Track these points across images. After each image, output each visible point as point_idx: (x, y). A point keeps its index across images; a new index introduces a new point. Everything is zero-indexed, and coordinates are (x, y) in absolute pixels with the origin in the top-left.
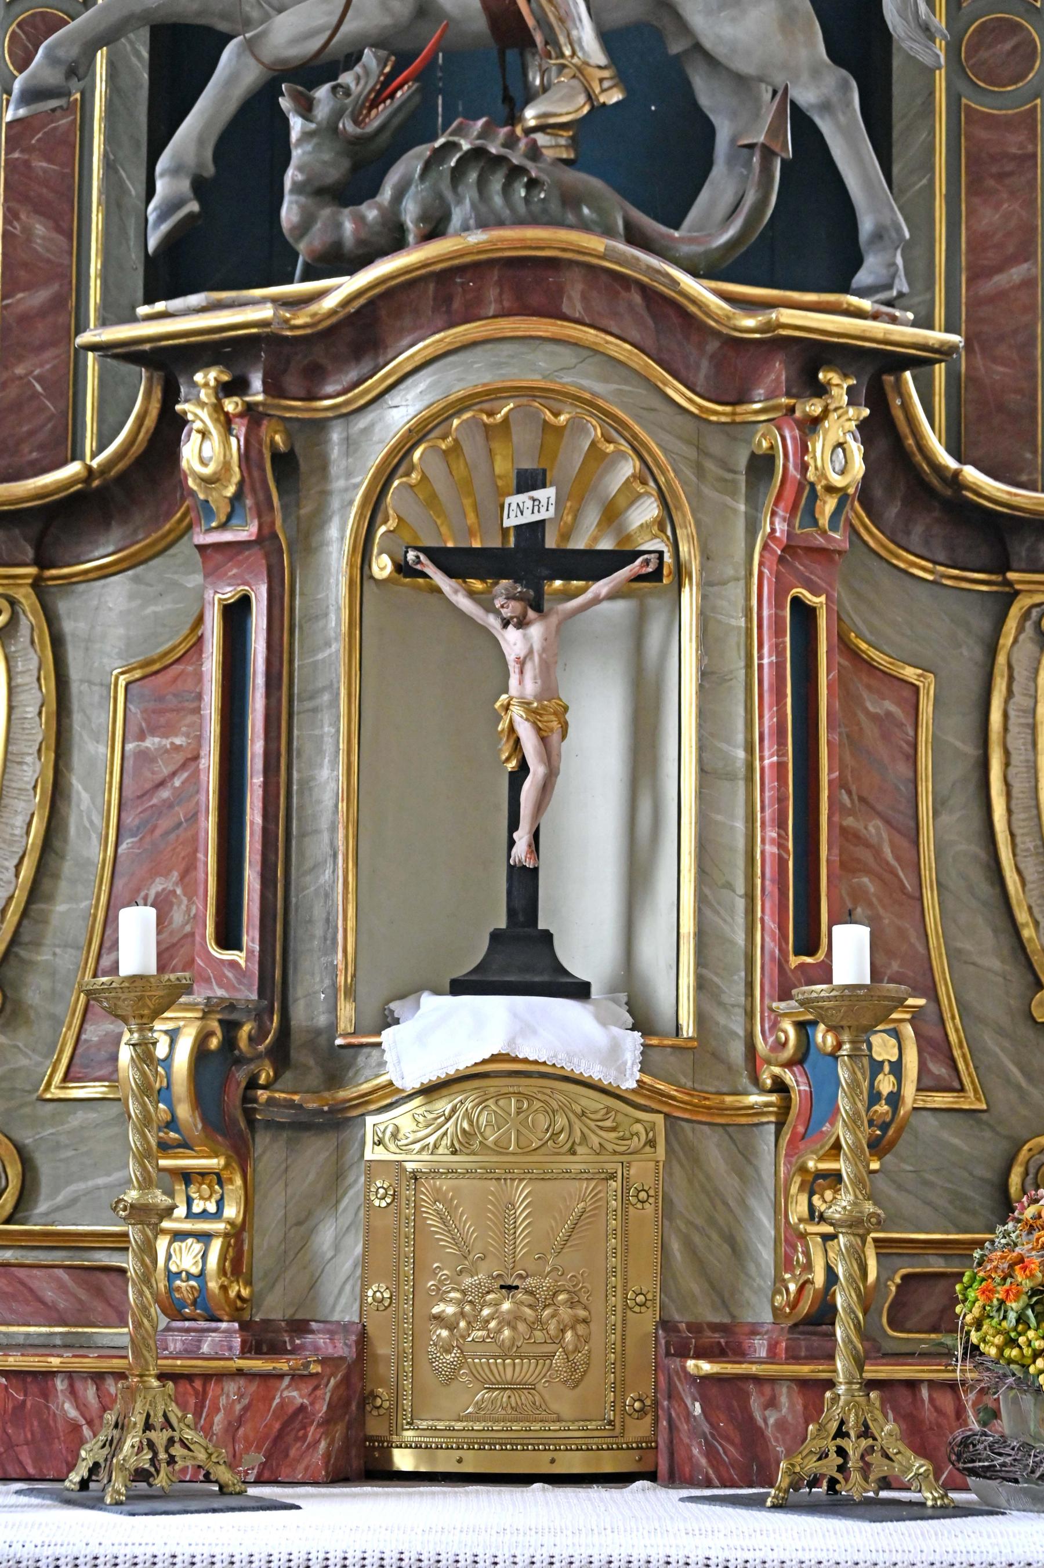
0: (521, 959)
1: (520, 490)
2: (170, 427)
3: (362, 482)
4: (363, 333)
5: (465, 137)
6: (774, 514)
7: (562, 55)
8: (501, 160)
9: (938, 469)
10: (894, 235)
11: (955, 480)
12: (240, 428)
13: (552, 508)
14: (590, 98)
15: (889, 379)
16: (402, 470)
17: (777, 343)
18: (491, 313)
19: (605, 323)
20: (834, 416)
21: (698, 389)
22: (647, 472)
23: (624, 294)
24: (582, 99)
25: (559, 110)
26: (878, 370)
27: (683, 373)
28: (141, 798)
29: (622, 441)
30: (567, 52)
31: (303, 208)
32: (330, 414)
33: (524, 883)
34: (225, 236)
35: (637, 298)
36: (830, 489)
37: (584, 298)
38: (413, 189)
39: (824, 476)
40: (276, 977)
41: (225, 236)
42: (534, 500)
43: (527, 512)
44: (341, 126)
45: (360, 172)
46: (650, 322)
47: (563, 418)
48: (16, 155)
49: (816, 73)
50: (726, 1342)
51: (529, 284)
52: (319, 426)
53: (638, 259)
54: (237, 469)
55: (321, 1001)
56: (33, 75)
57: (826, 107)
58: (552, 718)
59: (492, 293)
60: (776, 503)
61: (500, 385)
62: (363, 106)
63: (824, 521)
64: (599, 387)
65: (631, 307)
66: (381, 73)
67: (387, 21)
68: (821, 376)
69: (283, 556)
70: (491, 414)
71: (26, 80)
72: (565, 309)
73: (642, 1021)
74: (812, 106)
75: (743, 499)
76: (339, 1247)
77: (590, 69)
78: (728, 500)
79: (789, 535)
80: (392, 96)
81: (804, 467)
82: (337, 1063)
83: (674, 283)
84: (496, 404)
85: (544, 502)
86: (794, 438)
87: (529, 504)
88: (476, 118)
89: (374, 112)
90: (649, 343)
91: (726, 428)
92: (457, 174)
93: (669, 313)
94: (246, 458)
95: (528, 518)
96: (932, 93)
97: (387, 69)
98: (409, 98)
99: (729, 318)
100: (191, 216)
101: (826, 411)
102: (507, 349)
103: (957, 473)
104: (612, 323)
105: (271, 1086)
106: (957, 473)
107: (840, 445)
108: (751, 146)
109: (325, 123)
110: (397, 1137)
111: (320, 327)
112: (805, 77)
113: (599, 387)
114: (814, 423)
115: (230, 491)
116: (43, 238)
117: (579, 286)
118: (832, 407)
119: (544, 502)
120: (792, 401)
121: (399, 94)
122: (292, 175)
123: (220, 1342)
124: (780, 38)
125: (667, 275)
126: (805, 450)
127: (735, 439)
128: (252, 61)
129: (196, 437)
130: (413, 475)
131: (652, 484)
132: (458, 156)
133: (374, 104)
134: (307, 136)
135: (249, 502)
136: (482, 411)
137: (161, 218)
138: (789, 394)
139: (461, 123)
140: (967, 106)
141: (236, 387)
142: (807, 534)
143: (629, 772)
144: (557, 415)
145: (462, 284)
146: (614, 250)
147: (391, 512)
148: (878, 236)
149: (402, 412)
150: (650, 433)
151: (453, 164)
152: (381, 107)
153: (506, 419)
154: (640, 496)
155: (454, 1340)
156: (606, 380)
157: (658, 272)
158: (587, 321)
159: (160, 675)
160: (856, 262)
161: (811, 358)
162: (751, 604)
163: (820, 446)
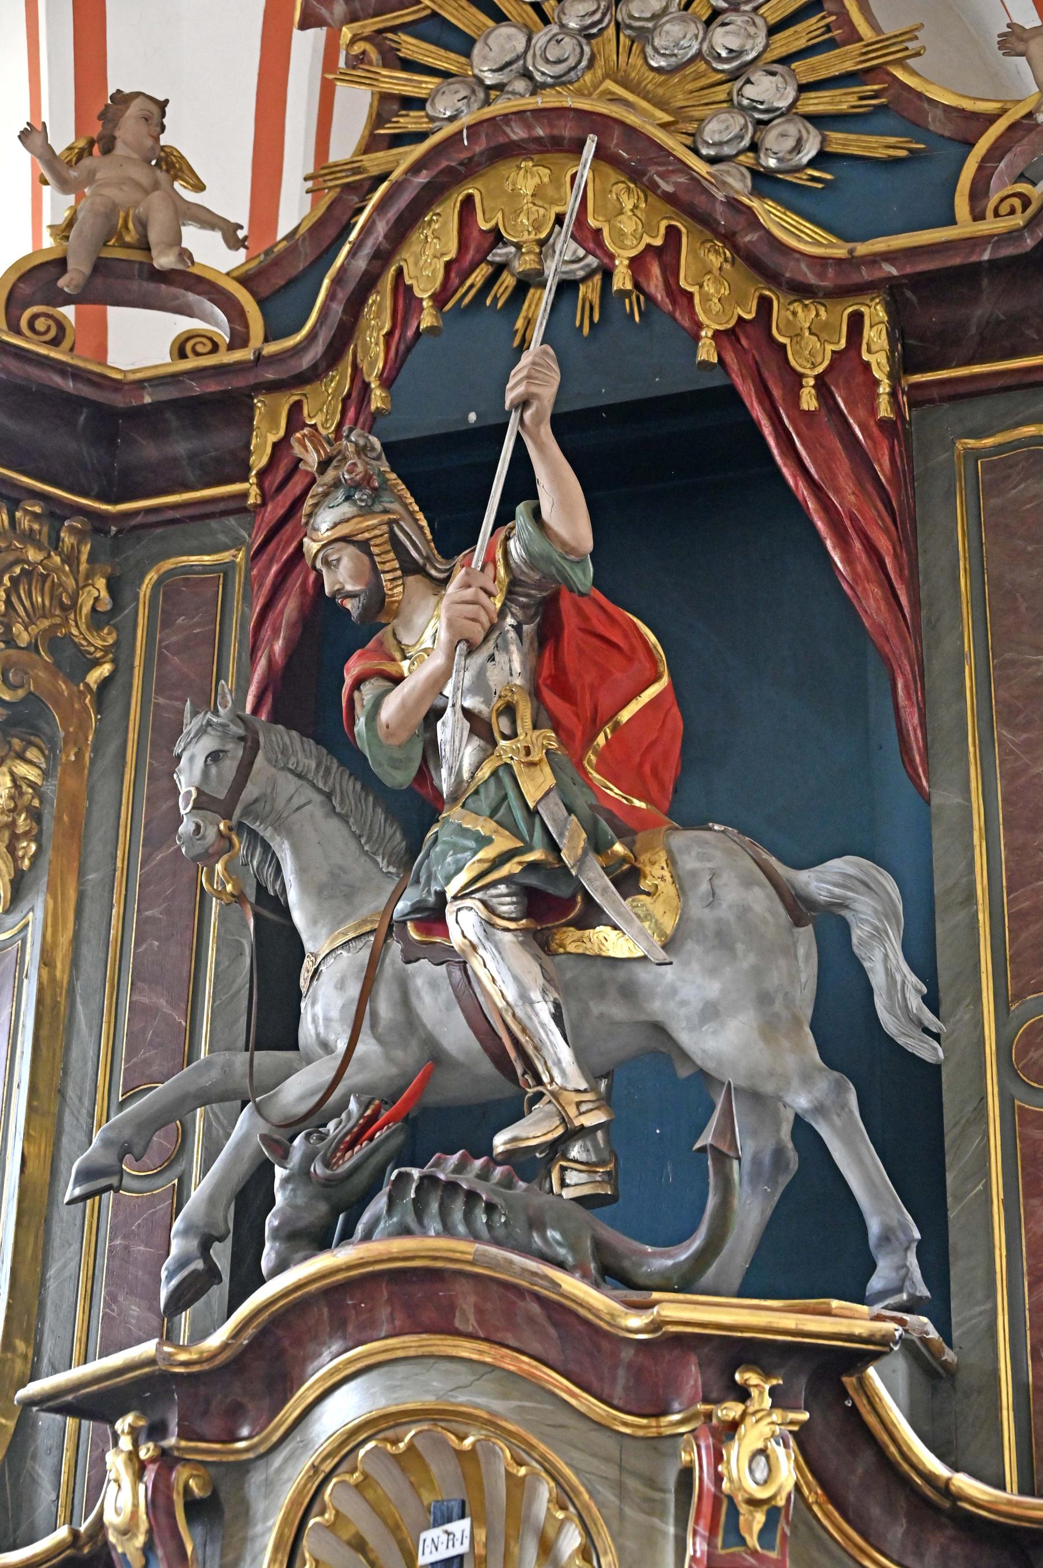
1: (436, 1524)
3: (274, 1524)
5: (443, 1171)
6: (695, 1533)
7: (539, 1082)
8: (452, 1187)
9: (929, 1478)
10: (901, 1236)
11: (945, 1489)
12: (150, 1476)
13: (467, 1542)
14: (563, 1121)
15: (849, 1381)
16: (316, 1508)
17: (675, 1343)
18: (383, 1334)
19: (499, 1336)
20: (750, 1420)
21: (616, 1402)
22: (565, 1497)
23: (521, 1304)
24: (557, 1121)
25: (524, 1135)
27: (596, 1385)
29: (534, 1464)
30: (546, 1079)
31: (278, 1254)
32: (251, 1455)
35: (535, 1308)
36: (754, 1503)
37: (479, 1311)
38: (382, 1225)
39: (741, 1488)
42: (448, 1533)
43: (442, 1547)
44: (312, 1169)
46: (552, 1332)
47: (468, 1443)
48: (118, 1242)
49: (807, 1078)
52: (242, 1469)
53: (511, 1262)
54: (144, 1517)
56: (88, 1156)
57: (819, 1109)
59: (384, 1313)
60: (696, 1522)
61: (393, 1409)
62: (337, 1149)
63: (753, 1541)
64: (497, 1405)
65: (531, 1320)
66: (361, 1116)
67: (394, 1071)
68: (737, 1377)
70: (395, 1442)
71: (82, 1162)
72: (458, 1324)
74: (806, 1111)
75: (671, 1520)
77: (566, 1093)
78: (656, 1521)
79: (710, 1555)
80: (371, 1139)
81: (718, 1478)
83: (555, 1285)
84: (399, 1430)
85: (458, 1536)
86: (707, 1448)
87: (444, 1538)
88: (478, 1158)
89: (349, 1153)
90: (553, 1355)
91: (655, 1443)
92: (419, 1207)
94: (152, 1505)
95: (443, 1554)
96: (983, 1098)
97: (368, 1112)
98: (387, 1138)
99: (612, 1315)
100: (194, 1272)
101: (744, 1415)
102: (401, 1369)
103: (948, 1481)
104: (509, 1335)
106: (948, 1481)
107: (762, 1451)
108: (703, 1149)
109: (297, 1167)
111: (217, 1362)
112: (795, 1082)
113: (497, 1405)
114: (733, 1427)
115: (140, 1540)
116: (138, 1318)
117: (472, 1299)
118: (751, 1410)
119: (458, 1536)
120: (709, 1407)
121: (378, 1134)
122: (271, 1221)
124: (761, 1044)
125: (545, 1277)
126: (718, 1458)
127: (664, 1455)
128: (261, 1121)
129: (113, 1486)
130: (327, 1516)
131: (572, 1509)
132: (414, 1186)
133: (351, 1146)
134: (286, 1181)
135: (160, 1552)
136: (386, 1440)
137: (170, 1278)
138: (706, 1400)
139: (439, 1158)
140: (1020, 1107)
141: (156, 1431)
142: (733, 1554)
144: (462, 1438)
145: (355, 1306)
146: (484, 1254)
147: (307, 1555)
148: (886, 1238)
150: (557, 1452)
151: (413, 1195)
152: (356, 1149)
153: (411, 1447)
154: (562, 1523)
156: (505, 1396)
157: (535, 1274)
158: (481, 1334)
160: (872, 1267)
163: (737, 1454)
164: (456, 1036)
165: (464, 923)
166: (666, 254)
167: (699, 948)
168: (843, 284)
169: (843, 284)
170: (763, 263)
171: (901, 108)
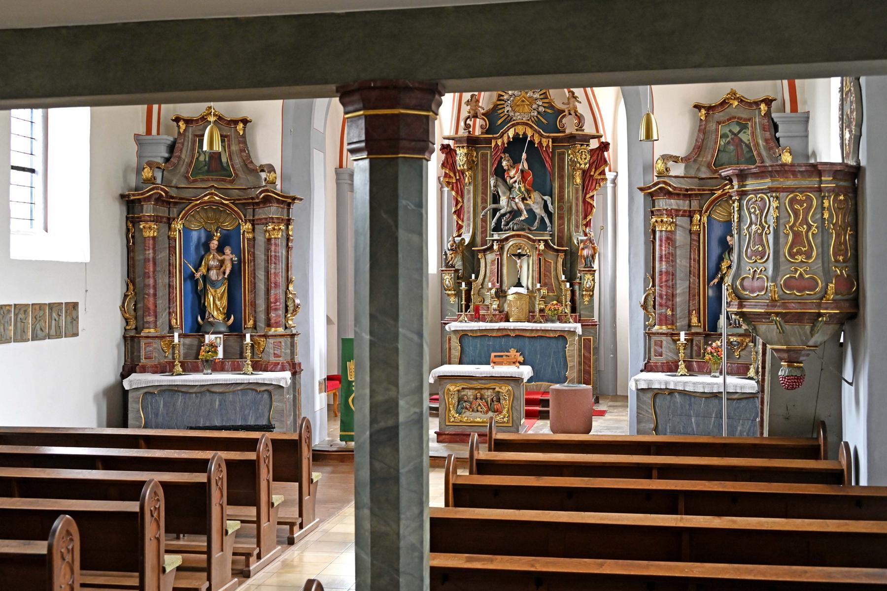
0: (519, 284)
2: (493, 245)
4: (507, 239)
26: (546, 241)
28: (491, 272)
33: (519, 279)
34: (497, 228)
40: (501, 286)
41: (497, 228)
45: (507, 224)
50: (533, 312)
51: (519, 236)
55: (505, 287)
58: (521, 267)
69: (501, 255)
73: (528, 289)
76: (506, 306)
82: (505, 292)
93: (529, 238)
105: (501, 294)
110: (510, 298)
123: (497, 312)
143: (527, 270)
149: (511, 243)
155: (514, 312)
159: (493, 262)
161: (539, 240)
162: (536, 258)
164: (515, 208)
165: (517, 200)
166: (533, 136)
167: (536, 202)
168: (548, 137)
169: (548, 137)
170: (541, 135)
171: (552, 107)
